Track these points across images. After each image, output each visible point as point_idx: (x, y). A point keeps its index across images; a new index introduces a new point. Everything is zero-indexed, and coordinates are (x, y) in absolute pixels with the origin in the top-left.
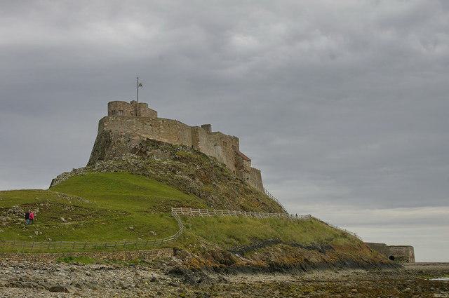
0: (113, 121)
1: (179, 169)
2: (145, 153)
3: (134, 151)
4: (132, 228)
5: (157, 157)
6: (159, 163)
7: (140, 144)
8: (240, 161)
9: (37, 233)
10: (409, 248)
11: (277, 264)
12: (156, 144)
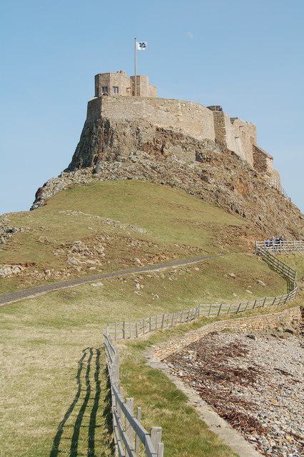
2: (162, 151)
4: (232, 275)
5: (180, 157)
6: (184, 167)
9: (138, 285)
12: (175, 137)
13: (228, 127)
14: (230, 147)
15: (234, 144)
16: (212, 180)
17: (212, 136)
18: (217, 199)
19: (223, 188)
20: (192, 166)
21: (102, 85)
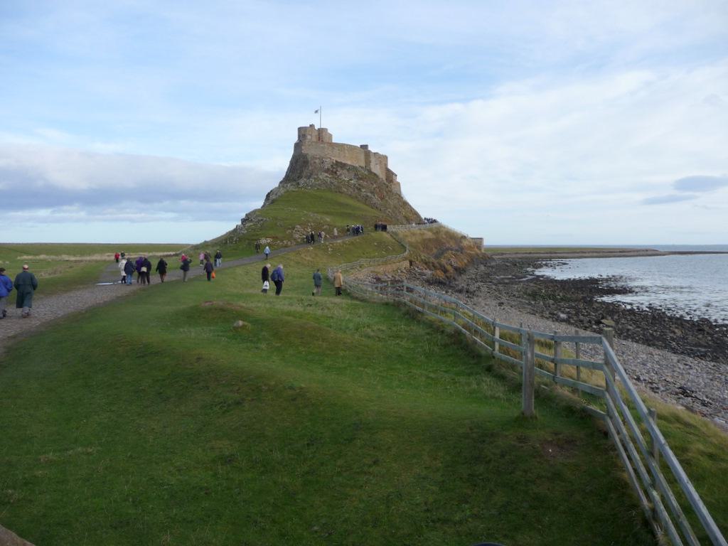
0: (309, 145)
1: (363, 187)
3: (327, 171)
7: (332, 166)
8: (390, 175)
10: (481, 239)
11: (460, 268)
12: (343, 166)
13: (373, 159)
14: (374, 170)
15: (376, 169)
16: (363, 190)
17: (363, 164)
18: (366, 200)
19: (369, 194)
20: (352, 182)
21: (302, 132)
